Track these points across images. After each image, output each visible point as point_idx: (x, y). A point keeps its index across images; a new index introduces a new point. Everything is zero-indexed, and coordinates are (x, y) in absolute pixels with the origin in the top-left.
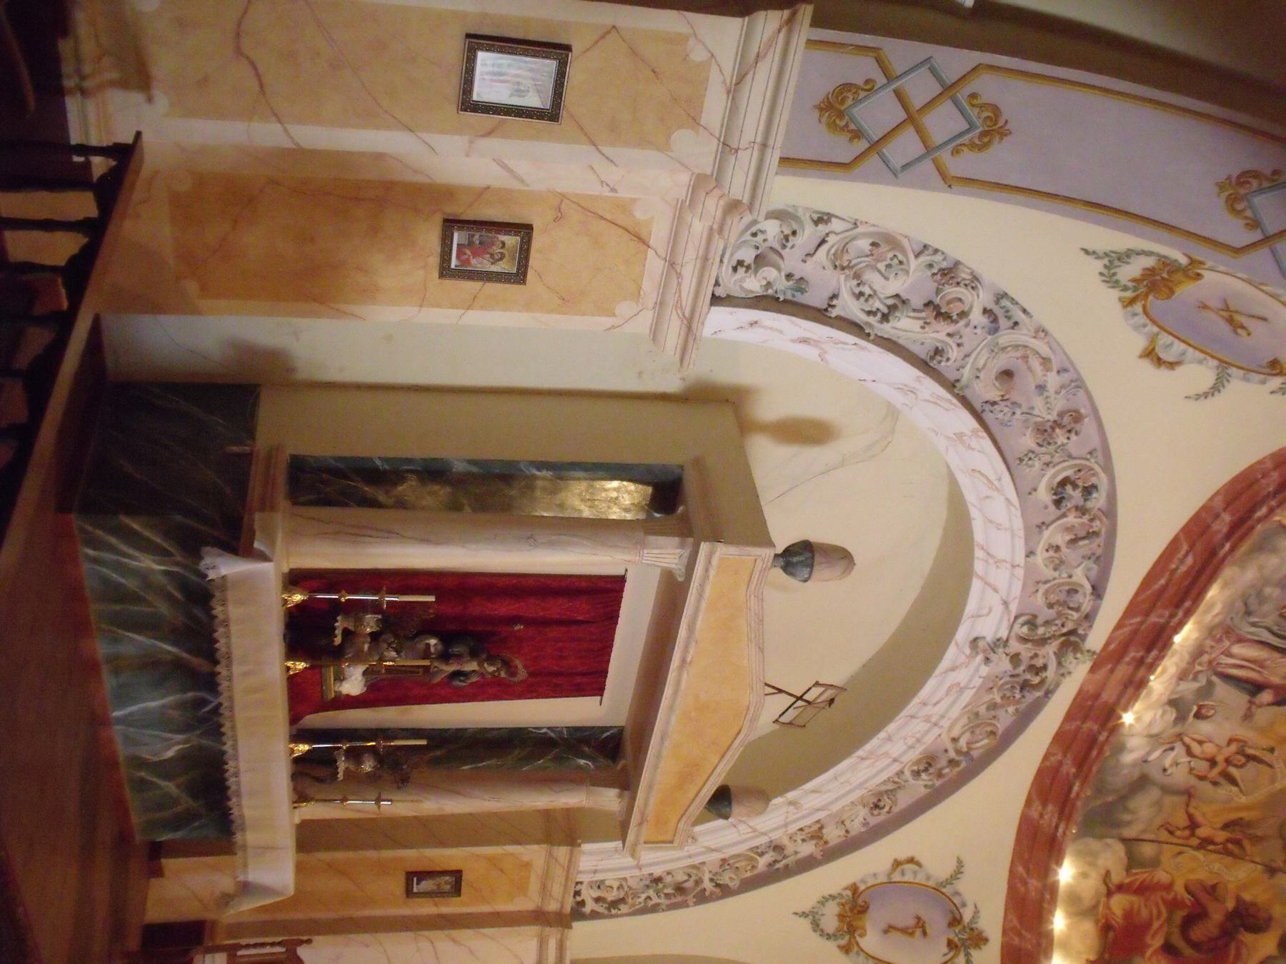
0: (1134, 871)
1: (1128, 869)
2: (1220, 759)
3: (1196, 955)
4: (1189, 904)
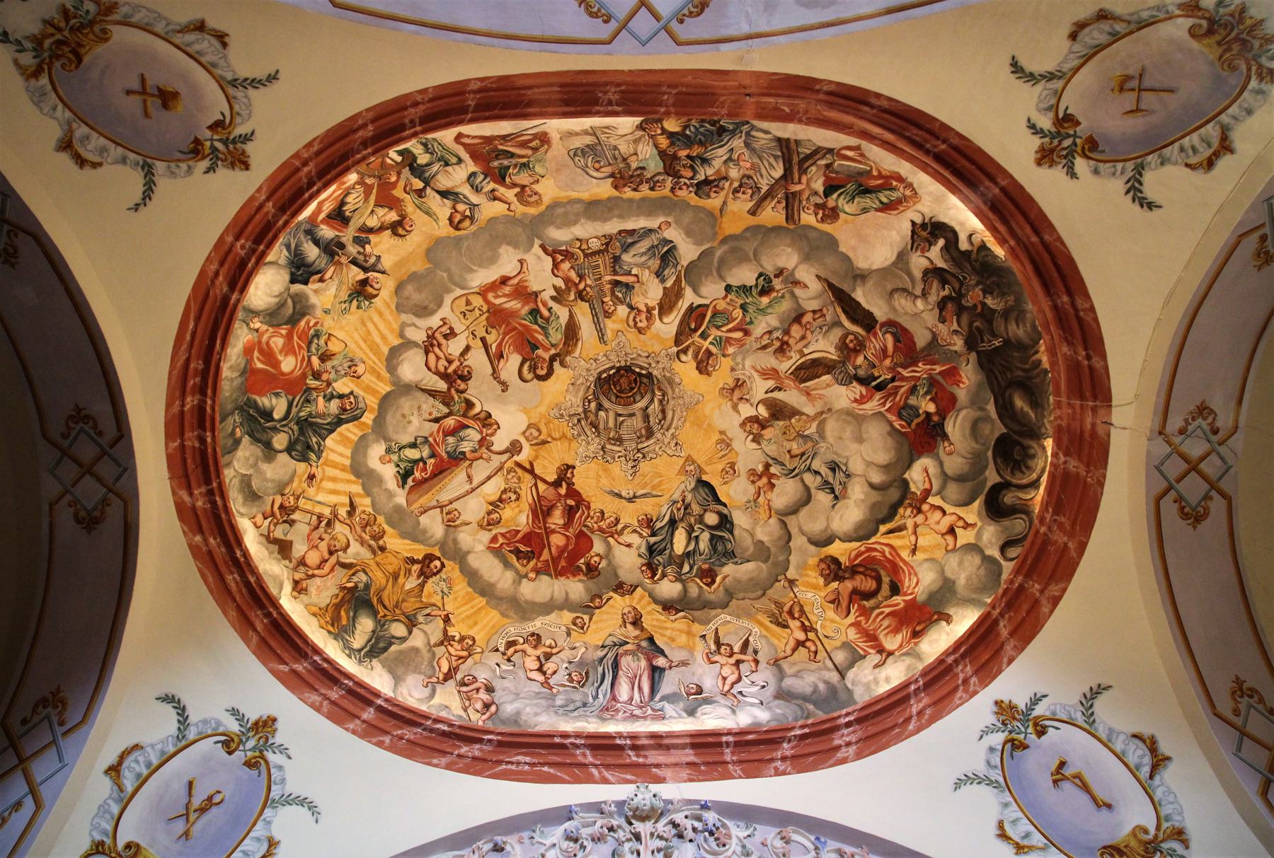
2: (732, 660)
3: (883, 573)
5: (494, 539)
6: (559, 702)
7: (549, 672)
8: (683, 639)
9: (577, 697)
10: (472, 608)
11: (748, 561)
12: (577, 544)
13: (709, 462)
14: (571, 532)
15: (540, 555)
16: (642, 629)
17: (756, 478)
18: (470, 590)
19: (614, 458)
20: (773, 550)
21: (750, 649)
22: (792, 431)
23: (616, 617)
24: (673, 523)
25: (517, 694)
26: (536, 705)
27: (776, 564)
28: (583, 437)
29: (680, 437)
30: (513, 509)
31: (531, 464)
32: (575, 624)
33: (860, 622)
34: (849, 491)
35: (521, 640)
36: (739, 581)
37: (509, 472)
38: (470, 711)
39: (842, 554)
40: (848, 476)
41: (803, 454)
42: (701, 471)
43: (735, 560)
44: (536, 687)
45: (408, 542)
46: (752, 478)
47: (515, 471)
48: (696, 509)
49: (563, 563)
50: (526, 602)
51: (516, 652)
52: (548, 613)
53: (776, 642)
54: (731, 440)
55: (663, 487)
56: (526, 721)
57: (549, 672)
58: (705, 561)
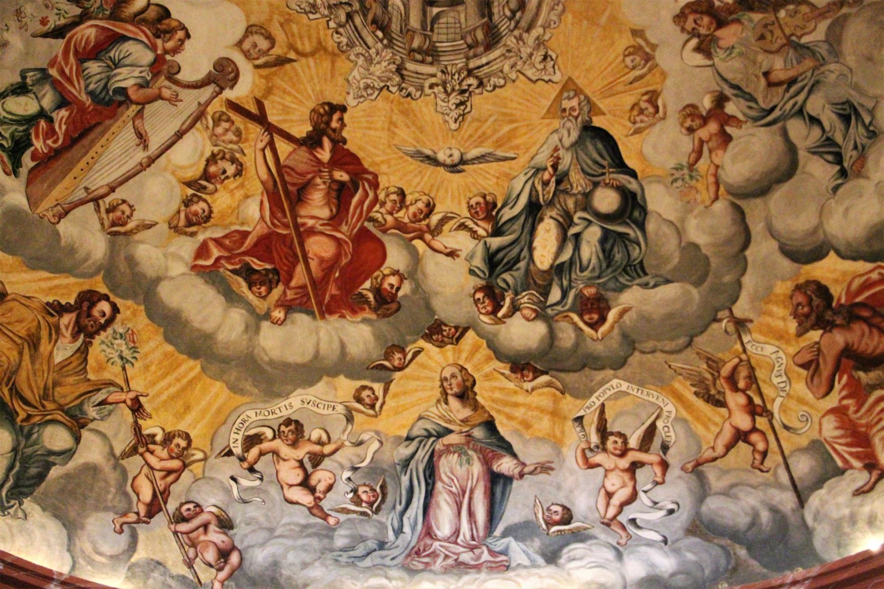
0: (840, 463)
1: (841, 472)
2: (624, 463)
4: (845, 378)
5: (202, 251)
6: (340, 542)
7: (321, 487)
8: (544, 424)
9: (369, 530)
10: (178, 380)
11: (668, 281)
12: (356, 252)
13: (609, 91)
14: (344, 232)
15: (290, 277)
16: (476, 406)
17: (698, 122)
18: (170, 348)
19: (421, 88)
20: (714, 262)
21: (656, 443)
22: (777, 32)
23: (429, 384)
24: (534, 210)
25: (271, 530)
26: (304, 548)
27: (715, 290)
28: (359, 49)
29: (553, 44)
30: (231, 192)
31: (260, 104)
32: (359, 400)
33: (846, 408)
34: (870, 164)
35: (269, 433)
36: (645, 319)
37: (217, 121)
38: (198, 565)
39: (836, 281)
40: (873, 135)
41: (792, 82)
42: (592, 108)
43: (645, 279)
44: (301, 516)
45: (45, 274)
46: (688, 123)
47: (229, 120)
48: (578, 182)
49: (333, 290)
50: (271, 363)
51: (262, 454)
52: (311, 383)
53: (699, 429)
54: (654, 47)
55: (518, 141)
56: (289, 578)
57: (321, 487)
58: (589, 282)
